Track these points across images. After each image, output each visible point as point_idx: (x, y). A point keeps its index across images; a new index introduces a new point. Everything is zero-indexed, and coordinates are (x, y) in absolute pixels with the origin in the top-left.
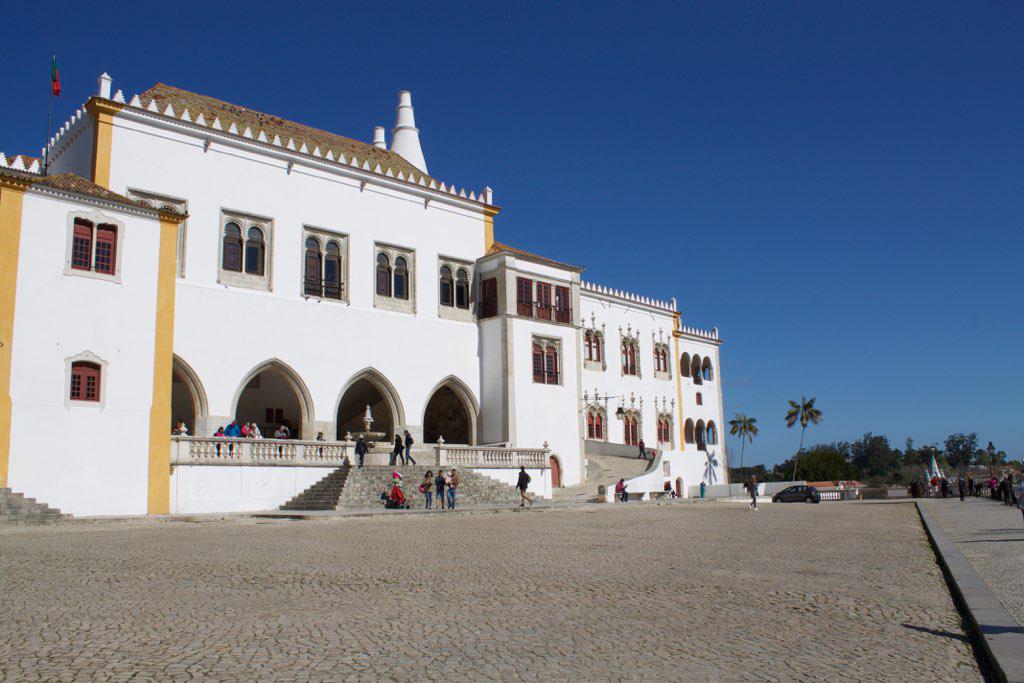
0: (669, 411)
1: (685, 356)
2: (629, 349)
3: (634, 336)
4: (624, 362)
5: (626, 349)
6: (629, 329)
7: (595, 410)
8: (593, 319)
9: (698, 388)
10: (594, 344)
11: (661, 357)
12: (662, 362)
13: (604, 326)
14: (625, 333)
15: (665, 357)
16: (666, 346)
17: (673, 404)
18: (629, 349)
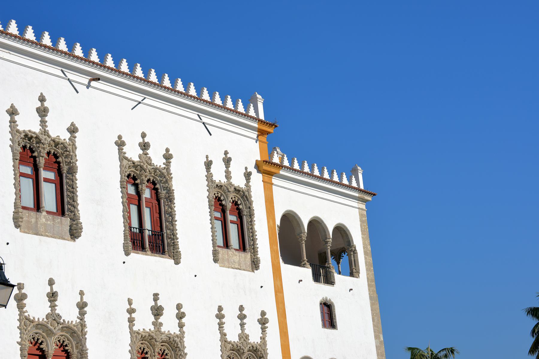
0: (255, 338)
1: (289, 220)
2: (147, 194)
3: (158, 161)
4: (135, 223)
5: (139, 194)
6: (145, 146)
7: (50, 333)
8: (43, 112)
9: (324, 291)
10: (44, 174)
11: (231, 218)
12: (233, 230)
13: (73, 130)
14: (133, 153)
15: (240, 217)
16: (244, 195)
17: (263, 322)
18: (147, 194)
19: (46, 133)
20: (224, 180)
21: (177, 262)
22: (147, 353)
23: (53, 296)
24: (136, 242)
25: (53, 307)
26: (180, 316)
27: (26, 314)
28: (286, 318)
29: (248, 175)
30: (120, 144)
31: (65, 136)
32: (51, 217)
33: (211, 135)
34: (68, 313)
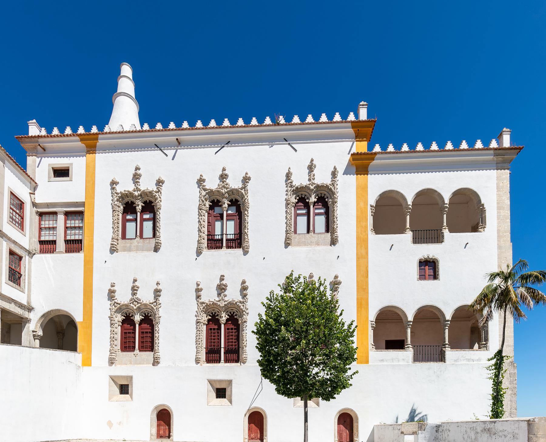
6: (223, 177)
9: (428, 250)
13: (160, 183)
14: (213, 184)
19: (138, 189)
20: (305, 182)
21: (246, 253)
22: (218, 315)
23: (134, 290)
24: (214, 243)
25: (134, 294)
26: (244, 288)
27: (116, 301)
28: (367, 277)
29: (334, 174)
30: (200, 182)
31: (152, 187)
32: (142, 240)
33: (296, 150)
34: (146, 296)
